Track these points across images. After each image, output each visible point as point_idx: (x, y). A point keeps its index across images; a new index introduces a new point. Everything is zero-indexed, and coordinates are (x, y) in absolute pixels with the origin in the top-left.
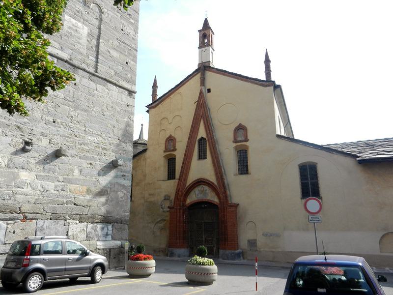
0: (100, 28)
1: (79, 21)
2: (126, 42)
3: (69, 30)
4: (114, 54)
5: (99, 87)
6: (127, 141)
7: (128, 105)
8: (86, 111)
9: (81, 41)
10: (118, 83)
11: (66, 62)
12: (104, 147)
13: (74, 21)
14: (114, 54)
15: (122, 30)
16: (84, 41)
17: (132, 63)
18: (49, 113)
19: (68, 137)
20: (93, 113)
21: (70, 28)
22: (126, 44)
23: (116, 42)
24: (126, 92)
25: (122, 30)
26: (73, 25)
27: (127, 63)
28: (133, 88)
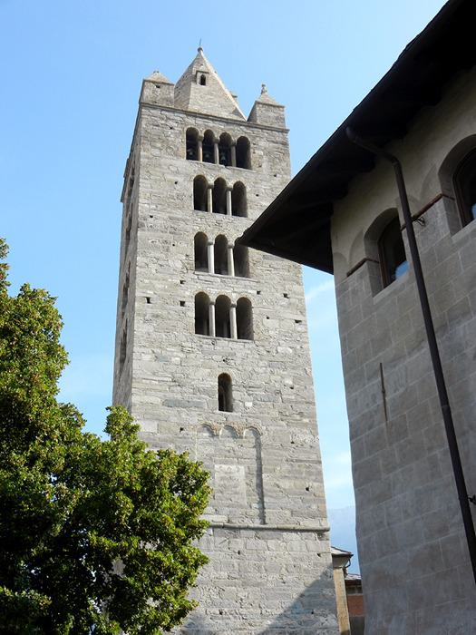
0: (259, 458)
1: (232, 463)
2: (301, 458)
3: (222, 483)
4: (286, 484)
5: (271, 543)
6: (327, 611)
7: (319, 555)
8: (258, 585)
9: (238, 490)
10: (298, 527)
11: (224, 527)
12: (292, 630)
13: (225, 467)
14: (286, 484)
15: (293, 443)
16: (243, 487)
17: (316, 484)
18: (213, 604)
19: (240, 629)
20: (269, 585)
21: (222, 479)
22: (301, 461)
23: (286, 467)
24: (314, 535)
25: (293, 443)
26: (226, 473)
27: (307, 489)
28: (325, 527)
